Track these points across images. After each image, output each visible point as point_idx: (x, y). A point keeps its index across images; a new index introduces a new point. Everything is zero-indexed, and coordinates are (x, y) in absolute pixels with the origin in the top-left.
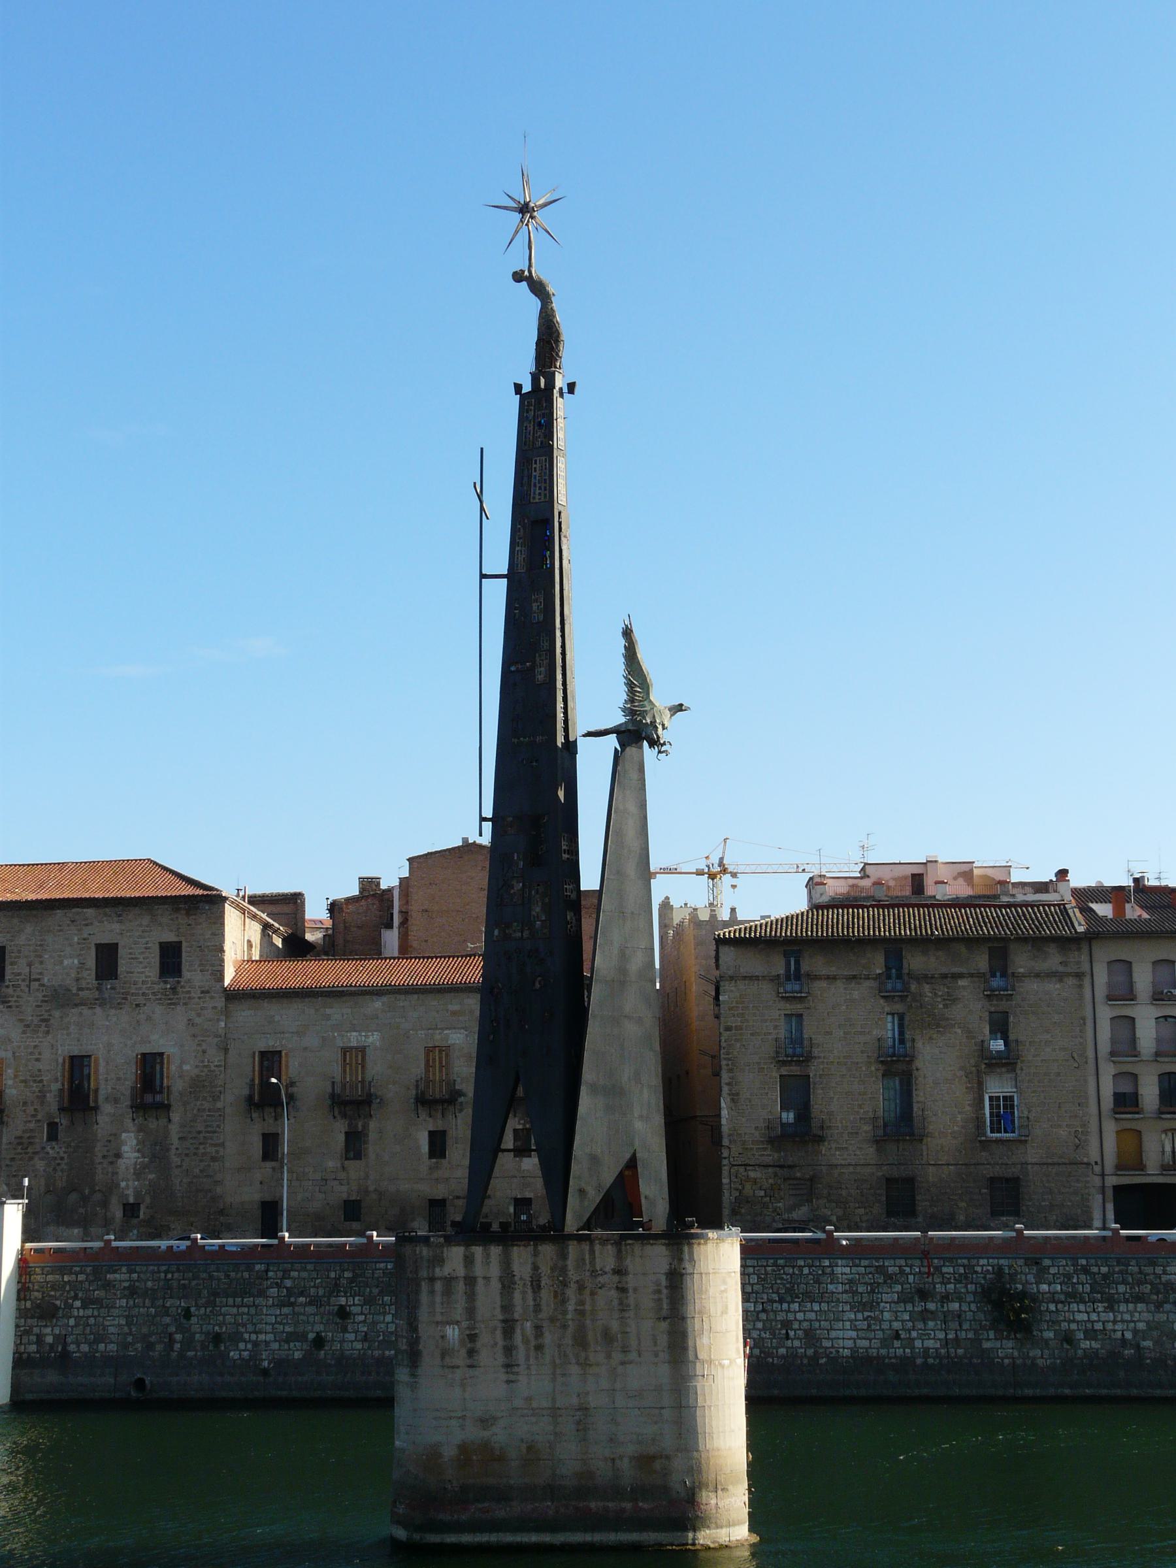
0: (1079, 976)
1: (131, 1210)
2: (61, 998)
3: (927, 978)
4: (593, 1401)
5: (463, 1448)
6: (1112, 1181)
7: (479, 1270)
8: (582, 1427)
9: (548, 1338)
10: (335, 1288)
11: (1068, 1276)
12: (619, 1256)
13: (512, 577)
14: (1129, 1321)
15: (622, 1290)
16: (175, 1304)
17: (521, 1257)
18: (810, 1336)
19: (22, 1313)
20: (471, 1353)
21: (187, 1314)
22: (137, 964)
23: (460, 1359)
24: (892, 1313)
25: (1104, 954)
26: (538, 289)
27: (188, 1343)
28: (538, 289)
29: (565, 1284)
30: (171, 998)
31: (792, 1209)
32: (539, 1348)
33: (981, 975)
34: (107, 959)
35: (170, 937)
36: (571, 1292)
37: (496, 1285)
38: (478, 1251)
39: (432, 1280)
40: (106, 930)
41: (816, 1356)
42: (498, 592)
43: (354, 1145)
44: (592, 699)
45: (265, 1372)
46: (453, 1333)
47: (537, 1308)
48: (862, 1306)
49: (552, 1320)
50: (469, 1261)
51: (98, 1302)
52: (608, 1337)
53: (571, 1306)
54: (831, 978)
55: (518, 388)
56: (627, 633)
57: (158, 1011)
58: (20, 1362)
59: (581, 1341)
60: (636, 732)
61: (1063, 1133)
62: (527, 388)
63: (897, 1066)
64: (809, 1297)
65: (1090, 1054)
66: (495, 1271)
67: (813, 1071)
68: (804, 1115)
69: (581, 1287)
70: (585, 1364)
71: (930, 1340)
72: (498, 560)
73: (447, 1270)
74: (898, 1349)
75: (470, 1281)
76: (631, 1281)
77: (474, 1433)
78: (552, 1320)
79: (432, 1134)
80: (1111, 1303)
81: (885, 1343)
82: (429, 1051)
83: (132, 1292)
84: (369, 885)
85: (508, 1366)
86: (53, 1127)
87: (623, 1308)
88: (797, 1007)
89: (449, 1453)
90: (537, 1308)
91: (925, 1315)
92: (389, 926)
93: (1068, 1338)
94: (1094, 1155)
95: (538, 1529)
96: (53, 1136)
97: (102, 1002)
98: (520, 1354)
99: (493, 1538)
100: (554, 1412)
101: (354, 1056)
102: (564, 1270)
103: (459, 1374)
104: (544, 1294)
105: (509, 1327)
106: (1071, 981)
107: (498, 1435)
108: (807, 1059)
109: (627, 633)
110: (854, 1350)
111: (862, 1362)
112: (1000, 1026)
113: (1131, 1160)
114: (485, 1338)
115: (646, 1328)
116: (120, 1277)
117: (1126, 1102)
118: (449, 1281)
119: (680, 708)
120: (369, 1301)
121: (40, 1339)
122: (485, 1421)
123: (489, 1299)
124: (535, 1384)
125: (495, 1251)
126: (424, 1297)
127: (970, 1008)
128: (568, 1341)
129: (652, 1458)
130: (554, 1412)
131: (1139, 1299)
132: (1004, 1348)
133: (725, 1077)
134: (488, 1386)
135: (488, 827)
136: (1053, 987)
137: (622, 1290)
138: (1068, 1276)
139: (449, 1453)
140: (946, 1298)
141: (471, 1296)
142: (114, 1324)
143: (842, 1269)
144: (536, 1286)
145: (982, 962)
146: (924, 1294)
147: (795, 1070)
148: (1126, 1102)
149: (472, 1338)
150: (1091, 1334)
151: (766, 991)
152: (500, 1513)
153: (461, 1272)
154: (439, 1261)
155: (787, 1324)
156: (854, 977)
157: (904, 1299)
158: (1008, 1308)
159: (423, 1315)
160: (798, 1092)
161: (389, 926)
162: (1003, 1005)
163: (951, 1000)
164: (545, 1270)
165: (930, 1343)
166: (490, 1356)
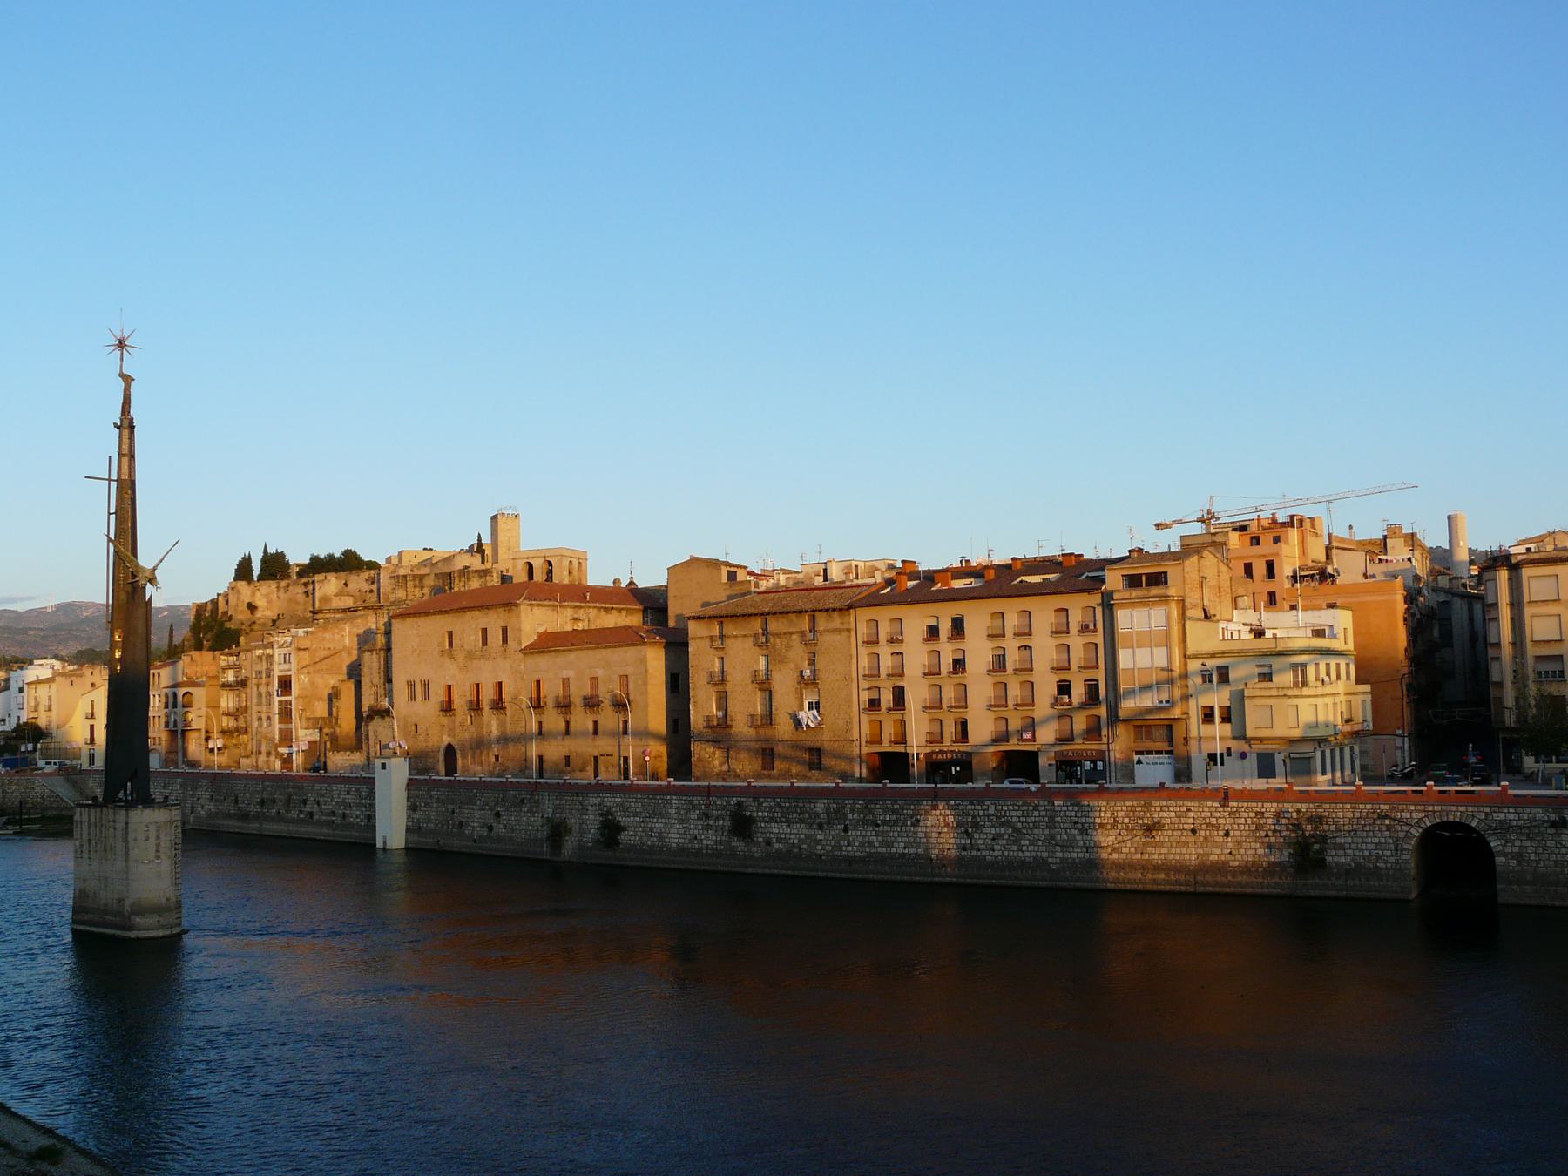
0: (849, 630)
2: (470, 656)
3: (778, 635)
6: (865, 750)
10: (497, 803)
14: (796, 833)
19: (409, 808)
24: (695, 826)
25: (865, 614)
26: (127, 379)
28: (127, 379)
33: (802, 633)
42: (113, 517)
48: (682, 821)
58: (407, 830)
61: (841, 723)
63: (764, 685)
64: (661, 815)
65: (854, 675)
66: (85, 818)
71: (710, 839)
74: (696, 845)
80: (789, 822)
81: (691, 841)
88: (721, 654)
91: (708, 827)
93: (768, 843)
94: (856, 736)
97: (482, 657)
101: (566, 682)
106: (845, 634)
108: (723, 681)
111: (681, 850)
112: (812, 662)
113: (876, 739)
115: (120, 846)
117: (874, 704)
127: (798, 654)
131: (801, 821)
132: (739, 845)
136: (836, 637)
140: (717, 818)
145: (805, 623)
146: (707, 816)
147: (720, 688)
148: (874, 704)
150: (779, 840)
151: (708, 642)
158: (742, 825)
162: (813, 649)
163: (789, 647)
166: (86, 855)
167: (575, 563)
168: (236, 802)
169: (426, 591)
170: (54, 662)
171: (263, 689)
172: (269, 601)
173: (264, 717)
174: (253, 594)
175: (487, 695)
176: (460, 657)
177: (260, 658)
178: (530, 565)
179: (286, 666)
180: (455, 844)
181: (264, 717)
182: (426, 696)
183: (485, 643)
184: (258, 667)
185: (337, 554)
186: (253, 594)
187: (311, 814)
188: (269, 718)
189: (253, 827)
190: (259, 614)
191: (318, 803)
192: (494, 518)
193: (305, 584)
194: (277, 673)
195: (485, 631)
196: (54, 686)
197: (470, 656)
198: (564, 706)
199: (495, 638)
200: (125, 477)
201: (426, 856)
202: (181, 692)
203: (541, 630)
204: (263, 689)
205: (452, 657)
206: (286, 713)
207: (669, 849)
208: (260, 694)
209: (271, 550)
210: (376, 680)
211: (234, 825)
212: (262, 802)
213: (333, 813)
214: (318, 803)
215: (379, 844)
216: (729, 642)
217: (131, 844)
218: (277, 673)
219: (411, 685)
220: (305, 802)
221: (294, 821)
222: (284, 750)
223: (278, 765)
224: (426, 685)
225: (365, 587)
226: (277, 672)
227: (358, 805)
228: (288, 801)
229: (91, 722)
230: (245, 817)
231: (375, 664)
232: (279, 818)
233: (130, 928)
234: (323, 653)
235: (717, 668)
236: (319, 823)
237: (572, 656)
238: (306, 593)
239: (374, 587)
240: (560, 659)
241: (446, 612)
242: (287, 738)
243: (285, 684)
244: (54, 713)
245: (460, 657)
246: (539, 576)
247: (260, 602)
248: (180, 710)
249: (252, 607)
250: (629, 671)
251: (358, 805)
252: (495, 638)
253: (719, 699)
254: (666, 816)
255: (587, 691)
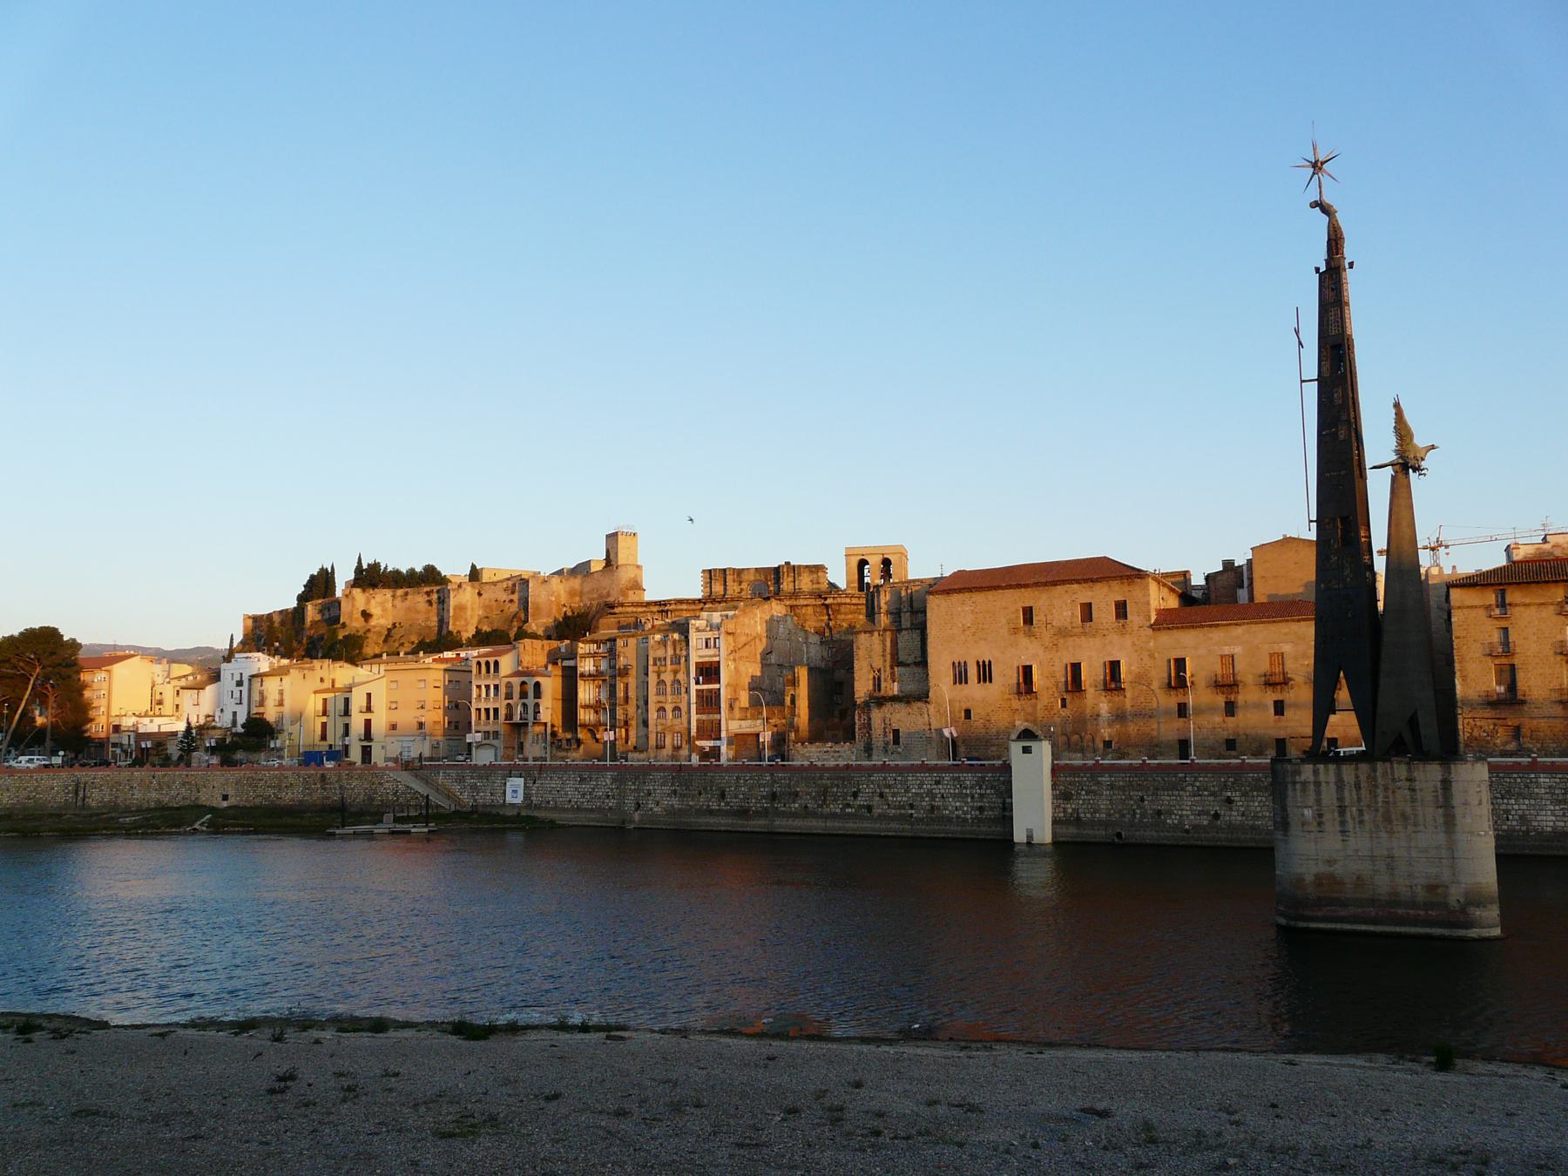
1: (1108, 744)
2: (1063, 633)
4: (1396, 853)
5: (1318, 877)
7: (1322, 777)
8: (1391, 869)
9: (1366, 817)
10: (1225, 787)
12: (1409, 770)
13: (1321, 380)
15: (1413, 790)
16: (1136, 794)
17: (1348, 772)
18: (1523, 819)
20: (1320, 824)
21: (1142, 800)
22: (1104, 613)
23: (1314, 827)
26: (1326, 209)
27: (1143, 815)
28: (1326, 209)
29: (1376, 786)
30: (1123, 631)
32: (1361, 822)
34: (1087, 612)
35: (1120, 598)
36: (1380, 791)
37: (1332, 786)
38: (1321, 767)
39: (1294, 783)
40: (1083, 594)
41: (1528, 831)
42: (1312, 390)
43: (1230, 709)
44: (1378, 446)
45: (1187, 831)
46: (1308, 813)
47: (1359, 800)
49: (1369, 806)
50: (1316, 772)
51: (1094, 792)
52: (1404, 816)
53: (1380, 799)
55: (1317, 270)
56: (1397, 405)
57: (1115, 637)
58: (1055, 822)
59: (1387, 819)
60: (1406, 464)
62: (1323, 269)
64: (1521, 795)
66: (1332, 778)
68: (1512, 687)
69: (1386, 789)
70: (1391, 832)
72: (1312, 371)
73: (1303, 778)
75: (1317, 784)
76: (1417, 785)
77: (1323, 868)
78: (1369, 806)
79: (1276, 702)
82: (1271, 655)
83: (1112, 787)
84: (1228, 565)
85: (1343, 832)
86: (1063, 700)
87: (1413, 800)
89: (1309, 878)
90: (1359, 800)
92: (1242, 586)
95: (1365, 923)
96: (1064, 705)
97: (1084, 634)
98: (1350, 826)
99: (1338, 926)
100: (1373, 858)
102: (1375, 779)
103: (1312, 836)
104: (1363, 792)
105: (1342, 810)
107: (1338, 869)
109: (1397, 405)
110: (1554, 828)
114: (1327, 817)
115: (1430, 814)
116: (1105, 779)
118: (1304, 784)
119: (1433, 447)
120: (1245, 794)
121: (1065, 811)
122: (1330, 862)
123: (1329, 795)
124: (1359, 842)
125: (1332, 767)
126: (1290, 792)
128: (1380, 818)
129: (1437, 887)
130: (1373, 858)
133: (1457, 666)
134: (1331, 843)
135: (1314, 525)
137: (1413, 790)
139: (1309, 878)
141: (1318, 793)
142: (1103, 804)
143: (1544, 779)
144: (1358, 786)
149: (1320, 816)
151: (1482, 613)
152: (1343, 913)
153: (1312, 779)
154: (1299, 773)
155: (1507, 812)
159: (1290, 801)
160: (1509, 675)
161: (1242, 586)
164: (1363, 778)
166: (1332, 826)
168: (723, 796)
169: (744, 586)
171: (668, 677)
172: (384, 610)
173: (669, 708)
174: (368, 601)
175: (1092, 674)
176: (1047, 636)
179: (711, 651)
180: (1149, 835)
181: (669, 708)
184: (660, 653)
185: (419, 569)
186: (368, 601)
187: (869, 808)
188: (677, 709)
189: (758, 824)
190: (373, 622)
191: (881, 795)
192: (612, 538)
193: (428, 593)
194: (694, 659)
196: (286, 679)
201: (1074, 850)
202: (531, 681)
204: (668, 677)
205: (1030, 635)
206: (709, 702)
207: (1540, 834)
208: (661, 682)
210: (878, 663)
211: (724, 823)
212: (773, 797)
213: (912, 806)
214: (881, 795)
215: (1019, 836)
216: (1516, 612)
217: (1458, 812)
220: (855, 795)
221: (833, 816)
222: (707, 744)
223: (695, 760)
225: (504, 596)
226: (698, 653)
227: (954, 796)
228: (824, 792)
229: (368, 716)
230: (743, 813)
231: (877, 647)
232: (806, 812)
233: (1470, 924)
234: (743, 639)
235: (1496, 637)
236: (883, 817)
237: (1239, 630)
238: (430, 603)
239: (515, 597)
240: (1217, 635)
241: (1026, 586)
242: (712, 731)
243: (710, 672)
244: (287, 708)
247: (375, 610)
248: (531, 701)
249: (366, 615)
251: (954, 796)
253: (1500, 670)
254: (1530, 796)
255: (1265, 666)
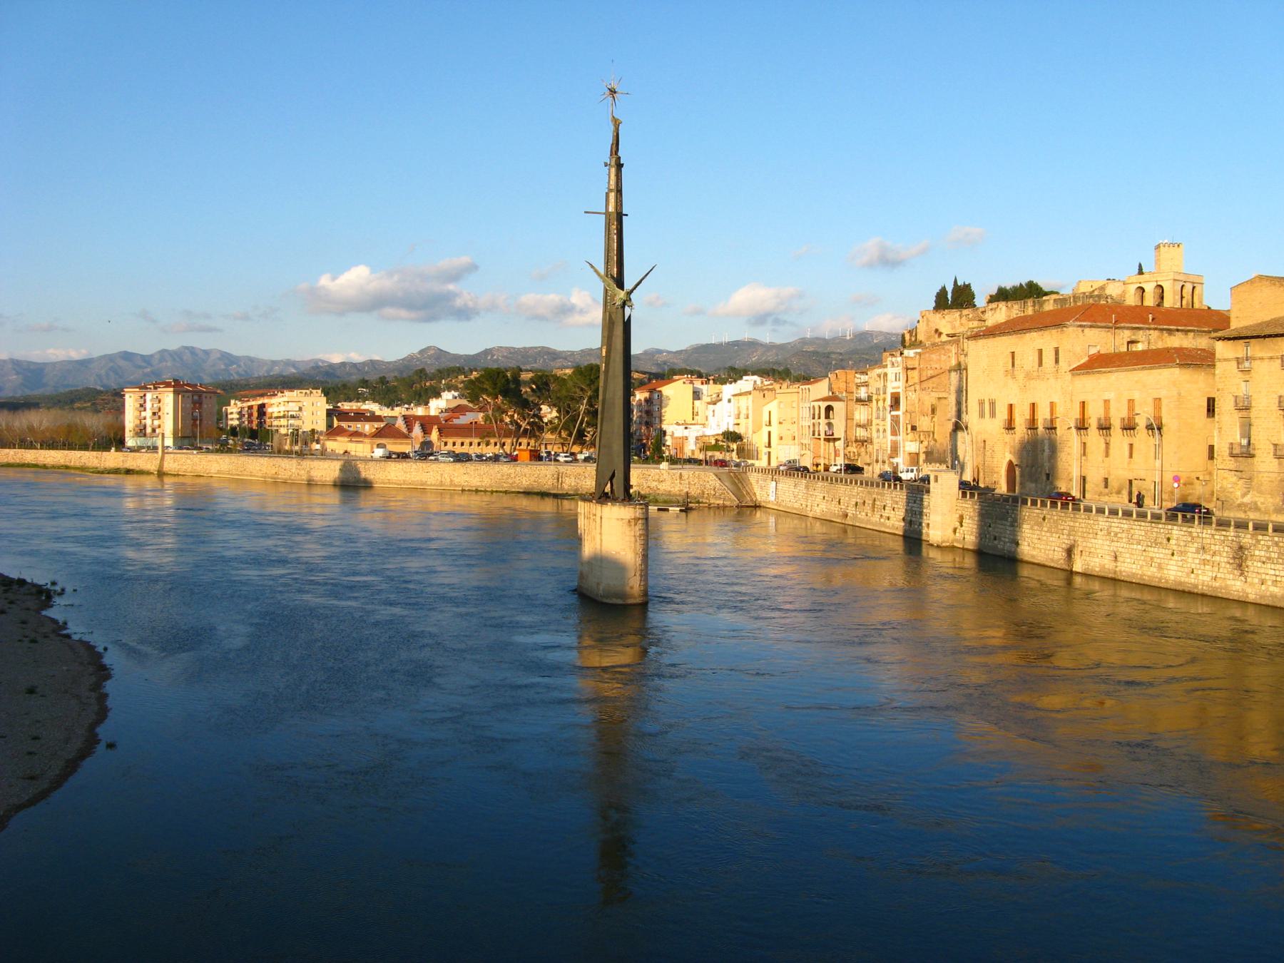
11: (1268, 547)
18: (1160, 567)
28: (617, 123)
31: (1244, 495)
54: (1261, 359)
57: (1052, 380)
67: (1253, 413)
68: (1249, 443)
91: (1205, 562)
101: (1107, 402)
108: (1247, 409)
138: (1268, 547)
140: (1214, 554)
147: (1244, 413)
151: (1234, 364)
156: (1271, 358)
157: (1197, 552)
165: (1205, 578)
167: (1189, 287)
170: (756, 378)
177: (879, 376)
178: (1142, 290)
182: (993, 414)
183: (1040, 364)
195: (1040, 351)
197: (1028, 376)
198: (1105, 428)
199: (1049, 358)
200: (611, 209)
203: (1093, 351)
209: (960, 283)
218: (890, 391)
219: (981, 403)
224: (992, 404)
229: (769, 429)
234: (930, 373)
245: (1020, 376)
246: (1150, 301)
250: (1162, 393)
252: (1049, 358)
